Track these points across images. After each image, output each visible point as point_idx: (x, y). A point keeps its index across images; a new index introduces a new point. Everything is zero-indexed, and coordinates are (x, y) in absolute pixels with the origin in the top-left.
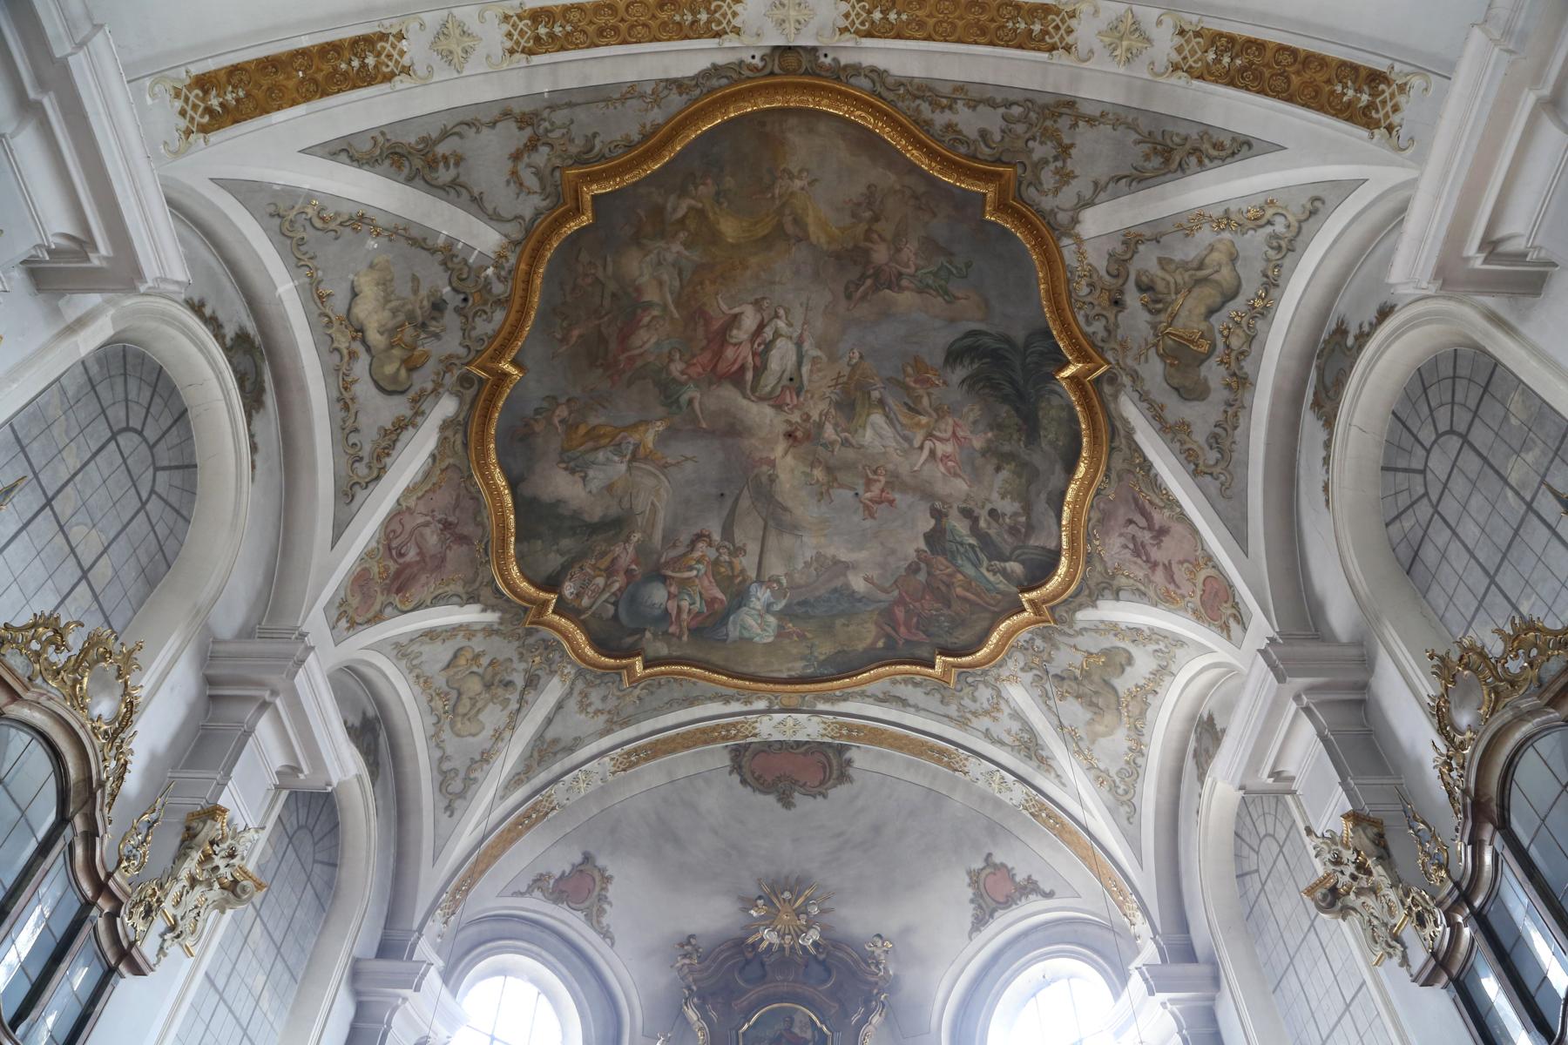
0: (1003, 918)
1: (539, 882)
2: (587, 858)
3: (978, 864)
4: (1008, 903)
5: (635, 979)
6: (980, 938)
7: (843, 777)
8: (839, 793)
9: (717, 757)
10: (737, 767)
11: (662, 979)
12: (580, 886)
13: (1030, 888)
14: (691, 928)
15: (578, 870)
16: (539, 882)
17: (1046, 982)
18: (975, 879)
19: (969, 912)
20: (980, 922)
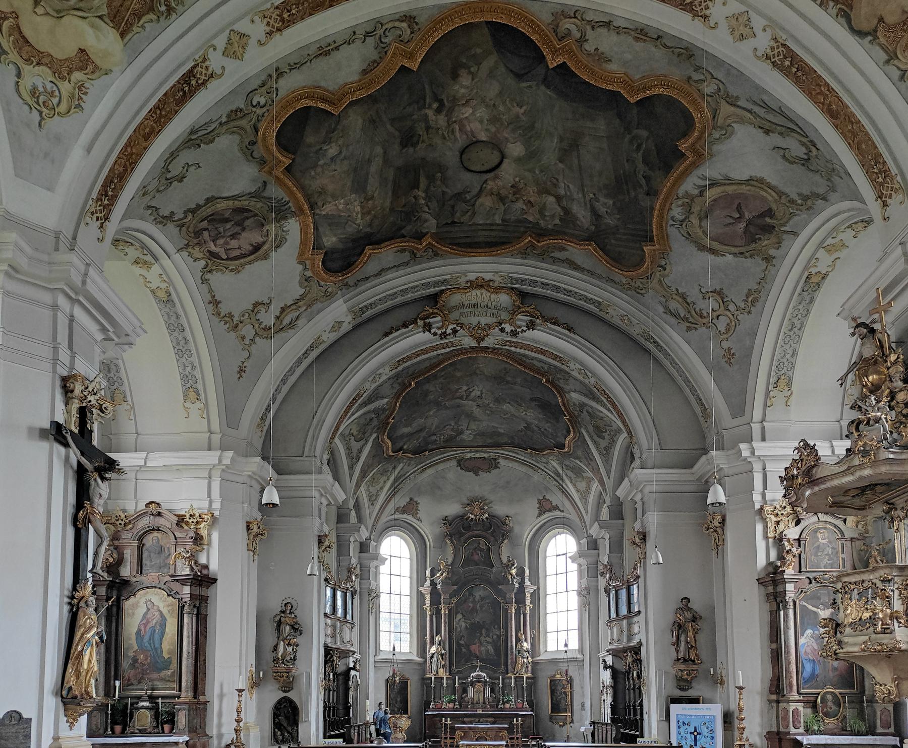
0: (547, 515)
1: (397, 510)
2: (411, 499)
3: (541, 498)
4: (549, 511)
5: (429, 531)
6: (540, 519)
7: (496, 467)
8: (495, 472)
9: (454, 463)
10: (459, 465)
11: (439, 529)
12: (411, 507)
13: (556, 508)
14: (446, 514)
15: (408, 503)
16: (397, 510)
17: (559, 533)
18: (539, 502)
19: (536, 512)
20: (540, 515)
